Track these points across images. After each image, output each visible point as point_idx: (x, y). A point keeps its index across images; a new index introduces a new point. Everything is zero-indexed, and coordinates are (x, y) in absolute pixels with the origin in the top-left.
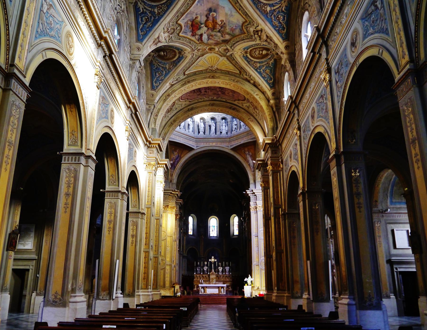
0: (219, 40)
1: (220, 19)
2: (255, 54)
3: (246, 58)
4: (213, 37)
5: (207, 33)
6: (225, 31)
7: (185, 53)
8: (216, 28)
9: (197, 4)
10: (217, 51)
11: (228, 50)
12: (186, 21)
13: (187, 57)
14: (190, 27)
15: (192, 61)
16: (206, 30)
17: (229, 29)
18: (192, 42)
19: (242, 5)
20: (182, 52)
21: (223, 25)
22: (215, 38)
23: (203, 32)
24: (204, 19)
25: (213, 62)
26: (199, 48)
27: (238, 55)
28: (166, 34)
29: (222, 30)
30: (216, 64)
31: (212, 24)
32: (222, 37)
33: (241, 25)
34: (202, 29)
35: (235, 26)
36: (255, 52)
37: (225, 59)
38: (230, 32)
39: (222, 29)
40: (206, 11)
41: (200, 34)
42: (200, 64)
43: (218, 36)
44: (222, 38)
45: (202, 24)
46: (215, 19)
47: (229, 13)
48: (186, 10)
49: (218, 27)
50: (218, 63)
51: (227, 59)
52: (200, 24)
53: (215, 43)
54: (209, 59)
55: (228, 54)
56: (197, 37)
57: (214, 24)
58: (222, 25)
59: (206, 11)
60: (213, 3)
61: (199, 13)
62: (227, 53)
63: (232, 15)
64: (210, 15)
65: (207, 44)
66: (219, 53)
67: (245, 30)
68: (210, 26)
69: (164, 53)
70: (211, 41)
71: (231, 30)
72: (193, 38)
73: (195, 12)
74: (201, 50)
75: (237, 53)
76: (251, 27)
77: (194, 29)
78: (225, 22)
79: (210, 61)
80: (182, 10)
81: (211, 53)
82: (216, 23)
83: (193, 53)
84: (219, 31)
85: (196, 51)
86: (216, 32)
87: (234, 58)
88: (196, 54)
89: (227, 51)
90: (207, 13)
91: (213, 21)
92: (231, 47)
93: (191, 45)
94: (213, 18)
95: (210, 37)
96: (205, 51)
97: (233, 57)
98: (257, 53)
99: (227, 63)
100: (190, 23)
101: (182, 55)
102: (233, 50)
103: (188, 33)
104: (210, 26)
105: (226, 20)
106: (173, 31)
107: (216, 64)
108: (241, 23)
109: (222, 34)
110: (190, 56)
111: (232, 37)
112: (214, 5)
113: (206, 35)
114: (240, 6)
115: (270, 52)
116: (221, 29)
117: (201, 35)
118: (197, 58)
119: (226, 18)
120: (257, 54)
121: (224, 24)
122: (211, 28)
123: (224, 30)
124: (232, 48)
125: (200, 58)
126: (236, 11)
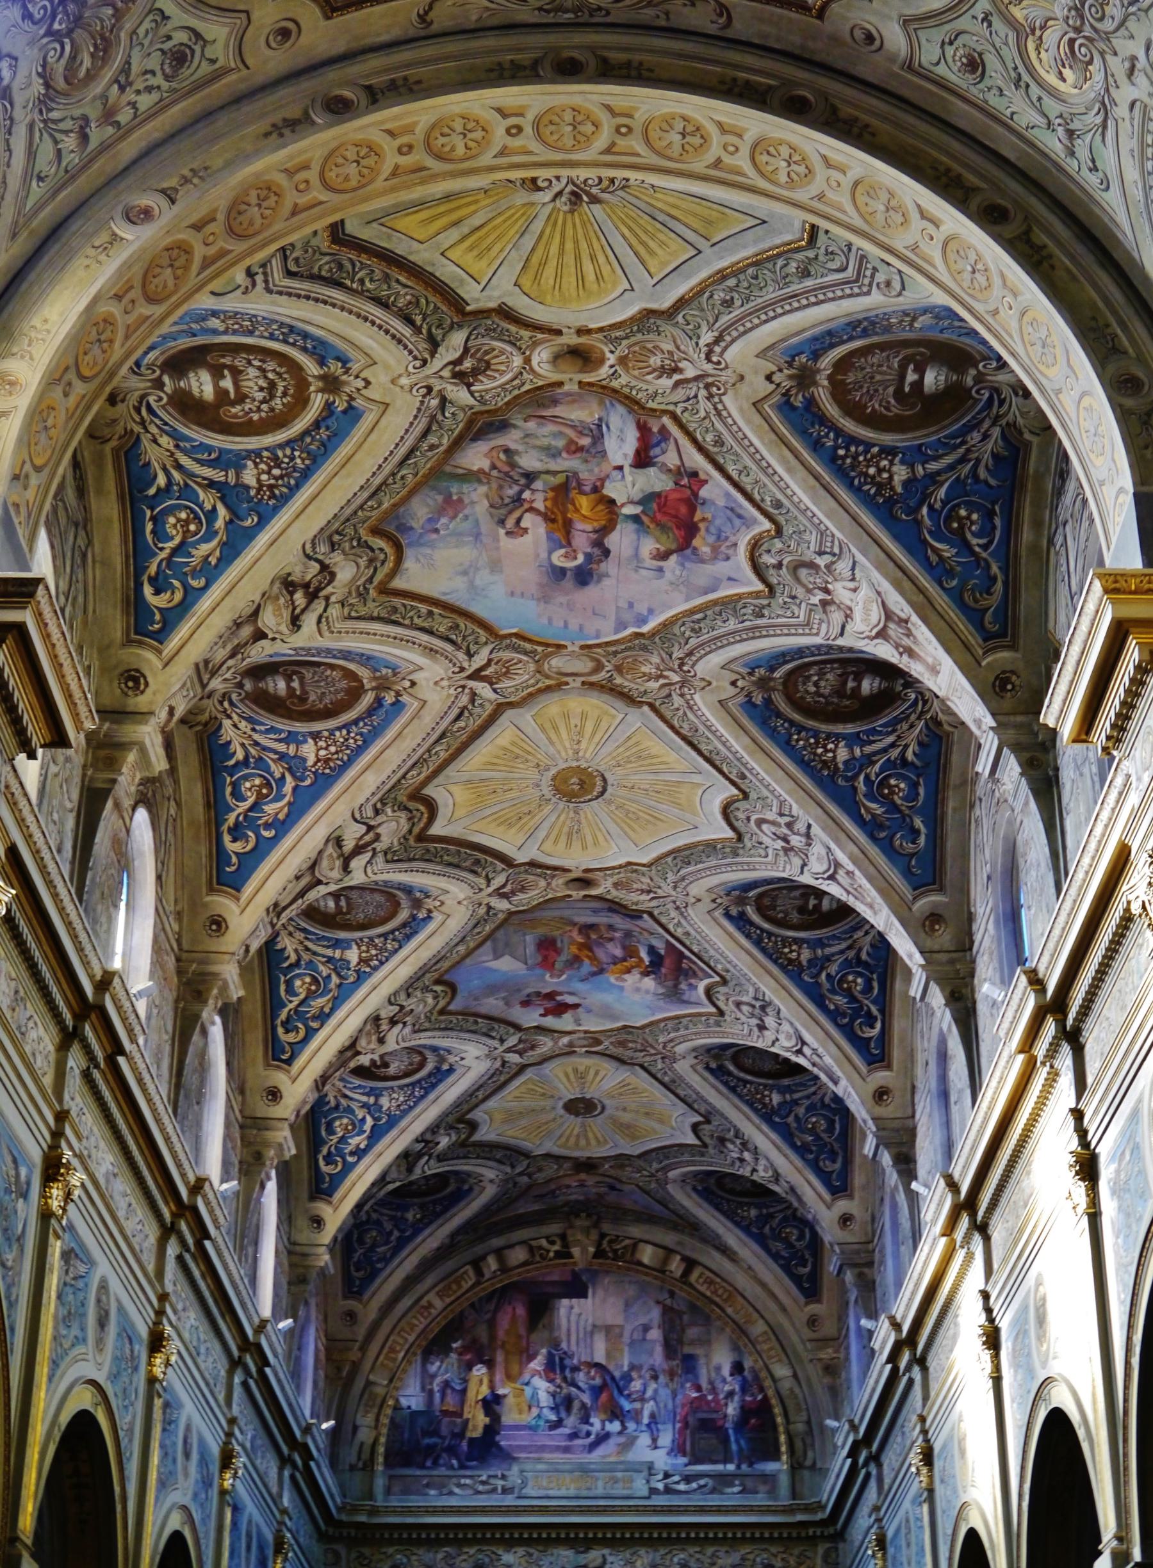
0: (531, 425)
1: (528, 538)
2: (263, 371)
3: (320, 351)
4: (571, 442)
5: (606, 468)
6: (494, 485)
7: (769, 378)
8: (551, 494)
9: (651, 611)
10: (535, 344)
11: (460, 377)
12: (721, 568)
13: (762, 354)
14: (702, 526)
15: (728, 303)
16: (607, 484)
17: (473, 503)
18: (709, 438)
19: (425, 638)
20: (787, 384)
21: (510, 512)
22: (555, 435)
23: (629, 478)
24: (621, 540)
25: (569, 245)
26: (666, 383)
27: (387, 367)
28: (841, 591)
29: (516, 488)
30: (537, 226)
31: (577, 510)
32: (513, 446)
33: (409, 553)
34: (636, 495)
35: (437, 531)
36: (272, 385)
37: (474, 295)
38: (466, 488)
39: (511, 491)
40: (607, 575)
41: (652, 471)
42: (675, 243)
43: (534, 453)
44: (510, 439)
45: (636, 519)
46: (558, 535)
47: (483, 577)
48: (709, 613)
49: (540, 497)
50: (528, 242)
51: (456, 303)
52: (645, 519)
53: (555, 402)
54: (599, 277)
55: (458, 338)
56: (671, 459)
57: (564, 513)
58: (516, 514)
59: (607, 575)
60: (570, 607)
61: (644, 572)
62: (466, 350)
63: (465, 573)
64: (589, 557)
65: (607, 393)
66: (525, 334)
67: (378, 543)
68: (584, 503)
69: (919, 384)
70: (584, 413)
71: (460, 500)
72: (697, 460)
73: (662, 584)
74: (655, 361)
75: (393, 381)
76: (354, 579)
77: (683, 510)
78: (502, 532)
79: (593, 258)
80: (732, 624)
81: (580, 332)
82: (548, 518)
83: (709, 367)
84: (530, 477)
85: (690, 373)
86: (548, 472)
87: (407, 331)
88: (688, 346)
89: (468, 364)
90: (603, 565)
91: (568, 525)
92: (444, 401)
93: (719, 426)
94: (569, 544)
95: (585, 441)
96: (622, 349)
97: (418, 330)
98: (252, 381)
99: (454, 254)
100: (701, 543)
101: (790, 364)
102: (429, 389)
103: (721, 502)
104: (584, 503)
105: (496, 539)
106: (803, 573)
107: (537, 226)
108: (409, 564)
109: (513, 465)
110: (709, 665)
111: (448, 469)
112: (563, 599)
113: (610, 454)
114: (429, 632)
115: (159, 384)
116: (521, 492)
117: (642, 460)
118: (691, 312)
119: (498, 548)
120: (252, 372)
121: (502, 522)
122: (582, 493)
123: (501, 487)
124: (435, 403)
125: (666, 304)
126: (443, 598)
